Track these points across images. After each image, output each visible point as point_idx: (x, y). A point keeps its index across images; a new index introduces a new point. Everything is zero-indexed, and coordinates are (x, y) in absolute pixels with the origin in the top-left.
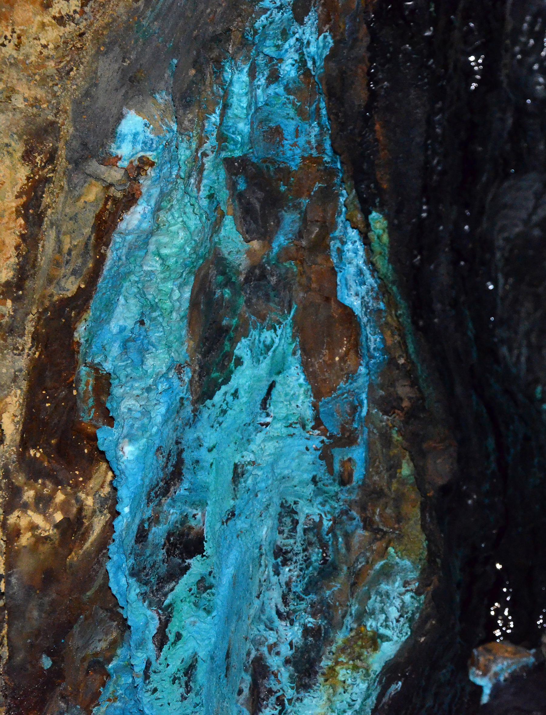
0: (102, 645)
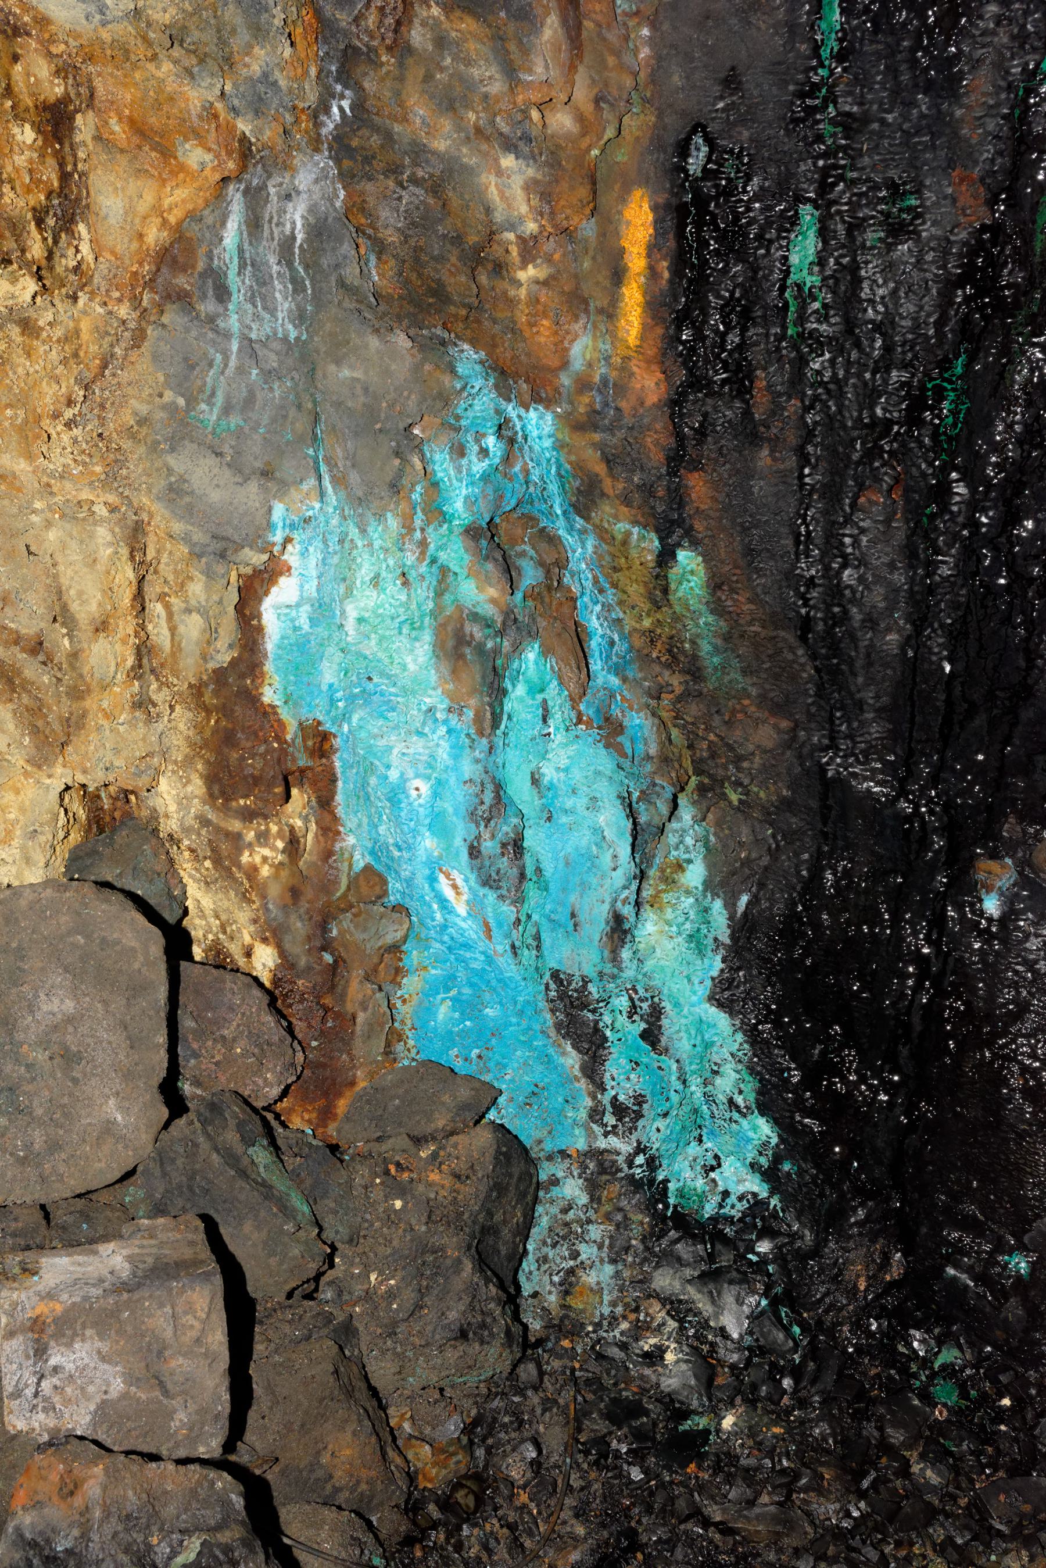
0: (399, 935)
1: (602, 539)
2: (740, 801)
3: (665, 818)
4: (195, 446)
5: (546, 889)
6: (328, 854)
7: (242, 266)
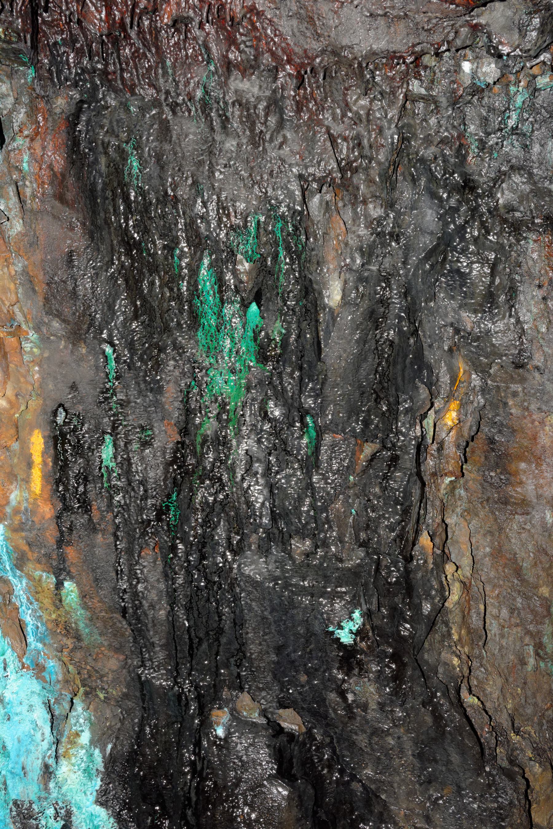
1: (29, 579)
2: (105, 697)
3: (68, 711)
5: (9, 757)
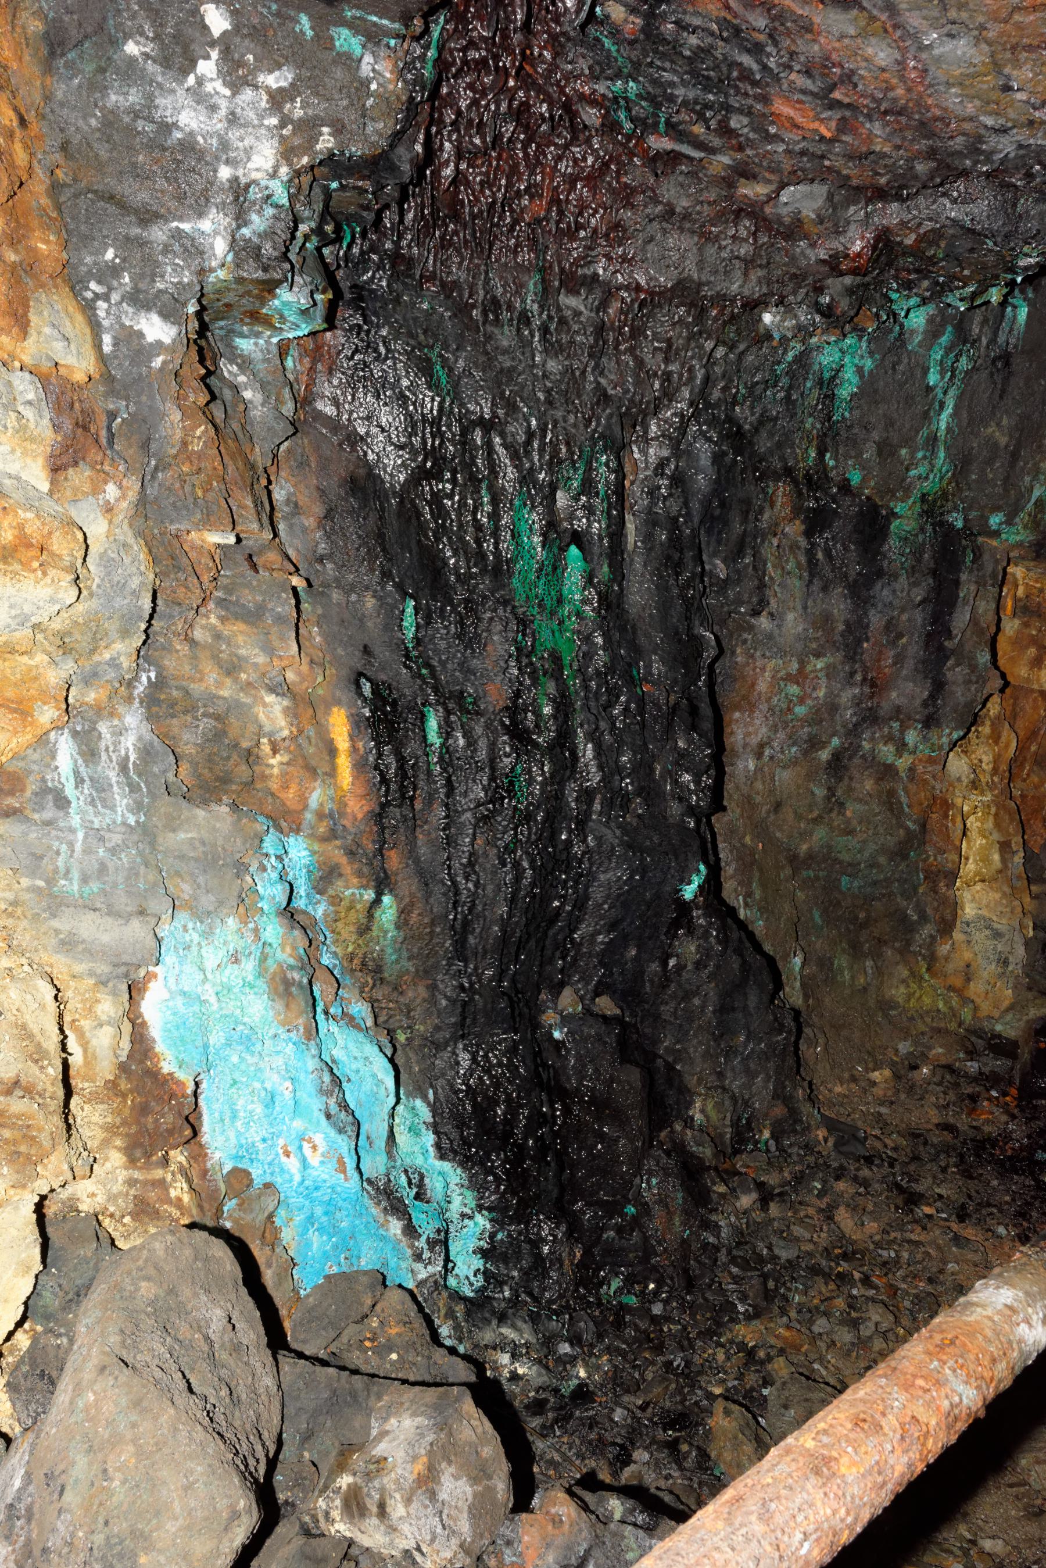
4: (72, 909)
6: (205, 1172)
7: (79, 781)
